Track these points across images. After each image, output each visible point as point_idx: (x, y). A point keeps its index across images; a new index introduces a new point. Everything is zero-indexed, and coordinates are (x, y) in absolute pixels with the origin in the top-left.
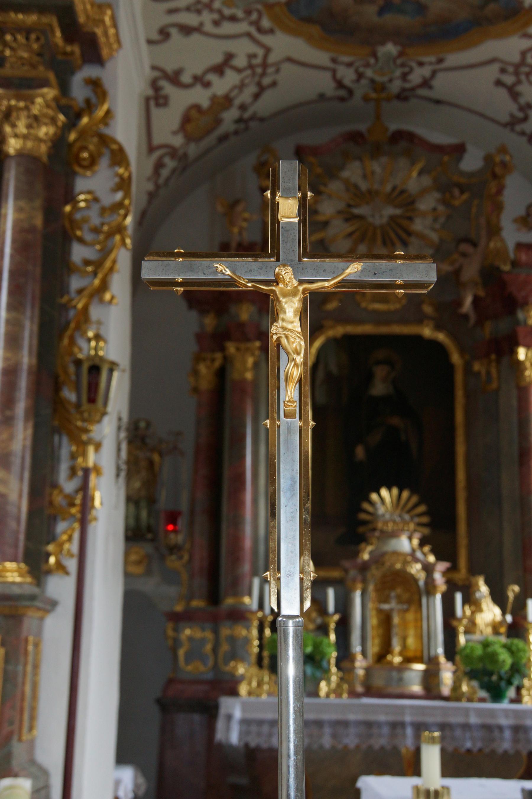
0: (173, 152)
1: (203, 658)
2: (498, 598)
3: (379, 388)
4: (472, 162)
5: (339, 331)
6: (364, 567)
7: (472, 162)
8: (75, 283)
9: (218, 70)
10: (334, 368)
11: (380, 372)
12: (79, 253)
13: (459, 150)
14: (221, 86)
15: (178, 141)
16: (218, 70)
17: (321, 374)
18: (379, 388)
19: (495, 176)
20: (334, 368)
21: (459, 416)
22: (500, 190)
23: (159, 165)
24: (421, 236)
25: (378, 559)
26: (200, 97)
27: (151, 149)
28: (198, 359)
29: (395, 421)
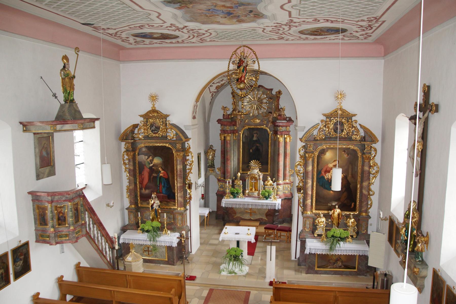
0: (215, 92)
1: (223, 188)
2: (272, 180)
3: (255, 139)
4: (274, 92)
5: (247, 127)
6: (248, 175)
7: (274, 92)
8: (188, 171)
9: (222, 81)
10: (246, 135)
11: (255, 135)
12: (188, 167)
13: (272, 90)
14: (222, 83)
15: (216, 90)
16: (222, 81)
17: (244, 136)
18: (255, 139)
19: (277, 97)
20: (246, 135)
21: (270, 144)
22: (278, 100)
23: (212, 95)
24: (264, 108)
25: (250, 174)
26: (219, 84)
27: (210, 93)
28: (220, 135)
29: (258, 145)
